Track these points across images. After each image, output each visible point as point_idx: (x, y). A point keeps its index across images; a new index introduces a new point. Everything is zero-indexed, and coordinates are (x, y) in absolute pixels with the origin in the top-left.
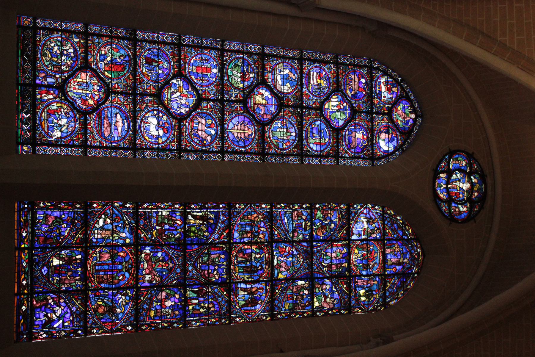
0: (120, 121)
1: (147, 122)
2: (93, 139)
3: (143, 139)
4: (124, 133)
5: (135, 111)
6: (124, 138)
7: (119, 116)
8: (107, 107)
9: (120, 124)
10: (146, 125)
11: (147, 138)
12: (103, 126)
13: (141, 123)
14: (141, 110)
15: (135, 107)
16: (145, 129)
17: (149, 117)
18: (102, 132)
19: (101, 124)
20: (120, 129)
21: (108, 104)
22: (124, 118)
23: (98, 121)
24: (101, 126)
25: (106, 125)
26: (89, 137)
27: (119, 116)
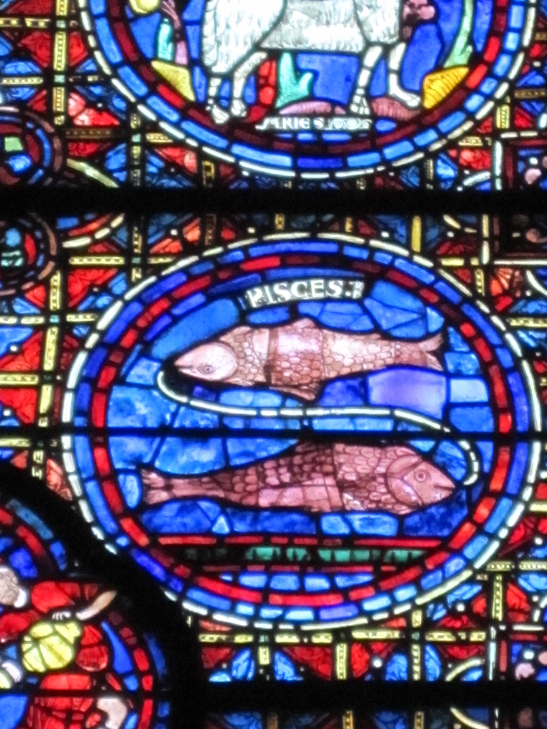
0: (260, 343)
1: (263, 80)
2: (484, 621)
3: (457, 127)
4: (395, 305)
5: (141, 203)
6: (456, 314)
7: (212, 361)
8: (106, 478)
9: (293, 343)
10: (292, 86)
11: (437, 88)
12: (333, 525)
13: (269, 142)
14: (121, 134)
15: (91, 201)
16: (341, 106)
17: (195, 63)
18: (403, 534)
19: (306, 542)
20: (348, 352)
21: (68, 469)
22: (225, 310)
23: (270, 568)
24: (323, 539)
25: (319, 492)
26: (470, 669)
27: (212, 361)
